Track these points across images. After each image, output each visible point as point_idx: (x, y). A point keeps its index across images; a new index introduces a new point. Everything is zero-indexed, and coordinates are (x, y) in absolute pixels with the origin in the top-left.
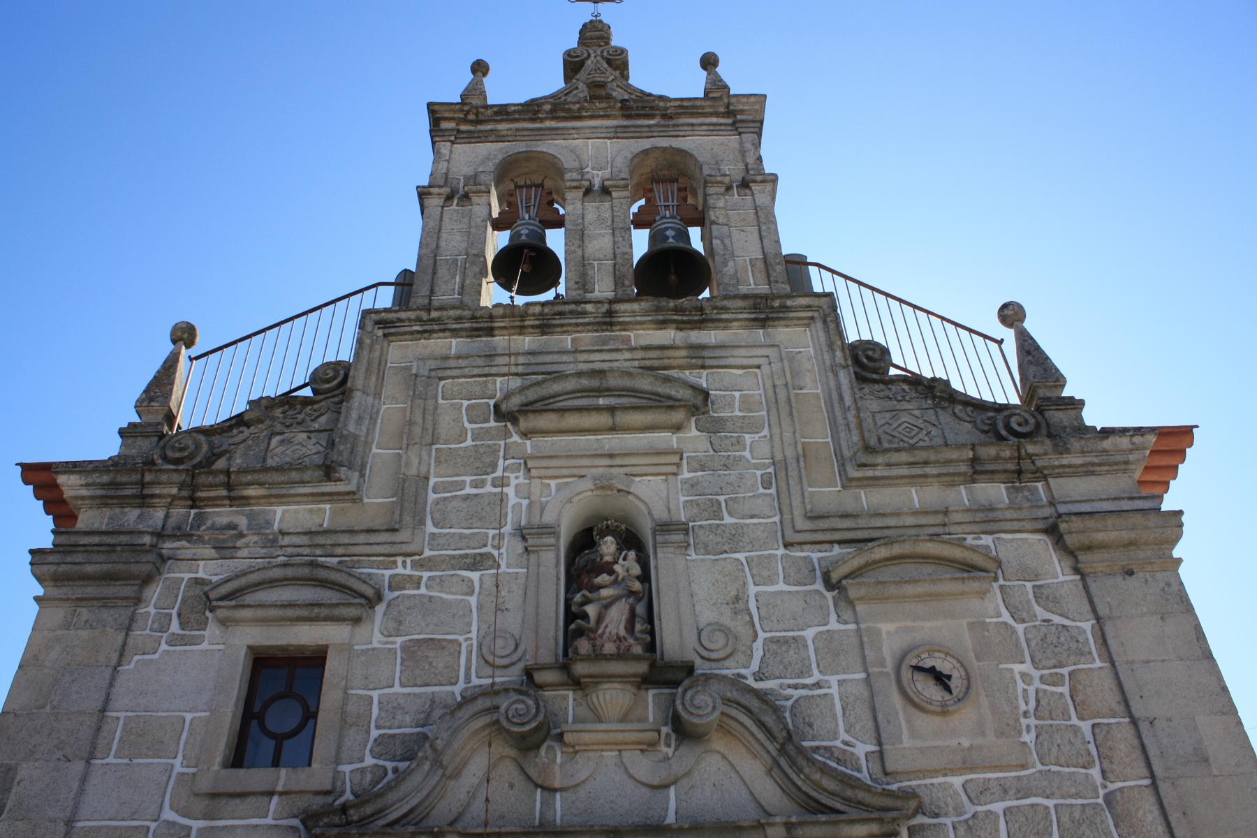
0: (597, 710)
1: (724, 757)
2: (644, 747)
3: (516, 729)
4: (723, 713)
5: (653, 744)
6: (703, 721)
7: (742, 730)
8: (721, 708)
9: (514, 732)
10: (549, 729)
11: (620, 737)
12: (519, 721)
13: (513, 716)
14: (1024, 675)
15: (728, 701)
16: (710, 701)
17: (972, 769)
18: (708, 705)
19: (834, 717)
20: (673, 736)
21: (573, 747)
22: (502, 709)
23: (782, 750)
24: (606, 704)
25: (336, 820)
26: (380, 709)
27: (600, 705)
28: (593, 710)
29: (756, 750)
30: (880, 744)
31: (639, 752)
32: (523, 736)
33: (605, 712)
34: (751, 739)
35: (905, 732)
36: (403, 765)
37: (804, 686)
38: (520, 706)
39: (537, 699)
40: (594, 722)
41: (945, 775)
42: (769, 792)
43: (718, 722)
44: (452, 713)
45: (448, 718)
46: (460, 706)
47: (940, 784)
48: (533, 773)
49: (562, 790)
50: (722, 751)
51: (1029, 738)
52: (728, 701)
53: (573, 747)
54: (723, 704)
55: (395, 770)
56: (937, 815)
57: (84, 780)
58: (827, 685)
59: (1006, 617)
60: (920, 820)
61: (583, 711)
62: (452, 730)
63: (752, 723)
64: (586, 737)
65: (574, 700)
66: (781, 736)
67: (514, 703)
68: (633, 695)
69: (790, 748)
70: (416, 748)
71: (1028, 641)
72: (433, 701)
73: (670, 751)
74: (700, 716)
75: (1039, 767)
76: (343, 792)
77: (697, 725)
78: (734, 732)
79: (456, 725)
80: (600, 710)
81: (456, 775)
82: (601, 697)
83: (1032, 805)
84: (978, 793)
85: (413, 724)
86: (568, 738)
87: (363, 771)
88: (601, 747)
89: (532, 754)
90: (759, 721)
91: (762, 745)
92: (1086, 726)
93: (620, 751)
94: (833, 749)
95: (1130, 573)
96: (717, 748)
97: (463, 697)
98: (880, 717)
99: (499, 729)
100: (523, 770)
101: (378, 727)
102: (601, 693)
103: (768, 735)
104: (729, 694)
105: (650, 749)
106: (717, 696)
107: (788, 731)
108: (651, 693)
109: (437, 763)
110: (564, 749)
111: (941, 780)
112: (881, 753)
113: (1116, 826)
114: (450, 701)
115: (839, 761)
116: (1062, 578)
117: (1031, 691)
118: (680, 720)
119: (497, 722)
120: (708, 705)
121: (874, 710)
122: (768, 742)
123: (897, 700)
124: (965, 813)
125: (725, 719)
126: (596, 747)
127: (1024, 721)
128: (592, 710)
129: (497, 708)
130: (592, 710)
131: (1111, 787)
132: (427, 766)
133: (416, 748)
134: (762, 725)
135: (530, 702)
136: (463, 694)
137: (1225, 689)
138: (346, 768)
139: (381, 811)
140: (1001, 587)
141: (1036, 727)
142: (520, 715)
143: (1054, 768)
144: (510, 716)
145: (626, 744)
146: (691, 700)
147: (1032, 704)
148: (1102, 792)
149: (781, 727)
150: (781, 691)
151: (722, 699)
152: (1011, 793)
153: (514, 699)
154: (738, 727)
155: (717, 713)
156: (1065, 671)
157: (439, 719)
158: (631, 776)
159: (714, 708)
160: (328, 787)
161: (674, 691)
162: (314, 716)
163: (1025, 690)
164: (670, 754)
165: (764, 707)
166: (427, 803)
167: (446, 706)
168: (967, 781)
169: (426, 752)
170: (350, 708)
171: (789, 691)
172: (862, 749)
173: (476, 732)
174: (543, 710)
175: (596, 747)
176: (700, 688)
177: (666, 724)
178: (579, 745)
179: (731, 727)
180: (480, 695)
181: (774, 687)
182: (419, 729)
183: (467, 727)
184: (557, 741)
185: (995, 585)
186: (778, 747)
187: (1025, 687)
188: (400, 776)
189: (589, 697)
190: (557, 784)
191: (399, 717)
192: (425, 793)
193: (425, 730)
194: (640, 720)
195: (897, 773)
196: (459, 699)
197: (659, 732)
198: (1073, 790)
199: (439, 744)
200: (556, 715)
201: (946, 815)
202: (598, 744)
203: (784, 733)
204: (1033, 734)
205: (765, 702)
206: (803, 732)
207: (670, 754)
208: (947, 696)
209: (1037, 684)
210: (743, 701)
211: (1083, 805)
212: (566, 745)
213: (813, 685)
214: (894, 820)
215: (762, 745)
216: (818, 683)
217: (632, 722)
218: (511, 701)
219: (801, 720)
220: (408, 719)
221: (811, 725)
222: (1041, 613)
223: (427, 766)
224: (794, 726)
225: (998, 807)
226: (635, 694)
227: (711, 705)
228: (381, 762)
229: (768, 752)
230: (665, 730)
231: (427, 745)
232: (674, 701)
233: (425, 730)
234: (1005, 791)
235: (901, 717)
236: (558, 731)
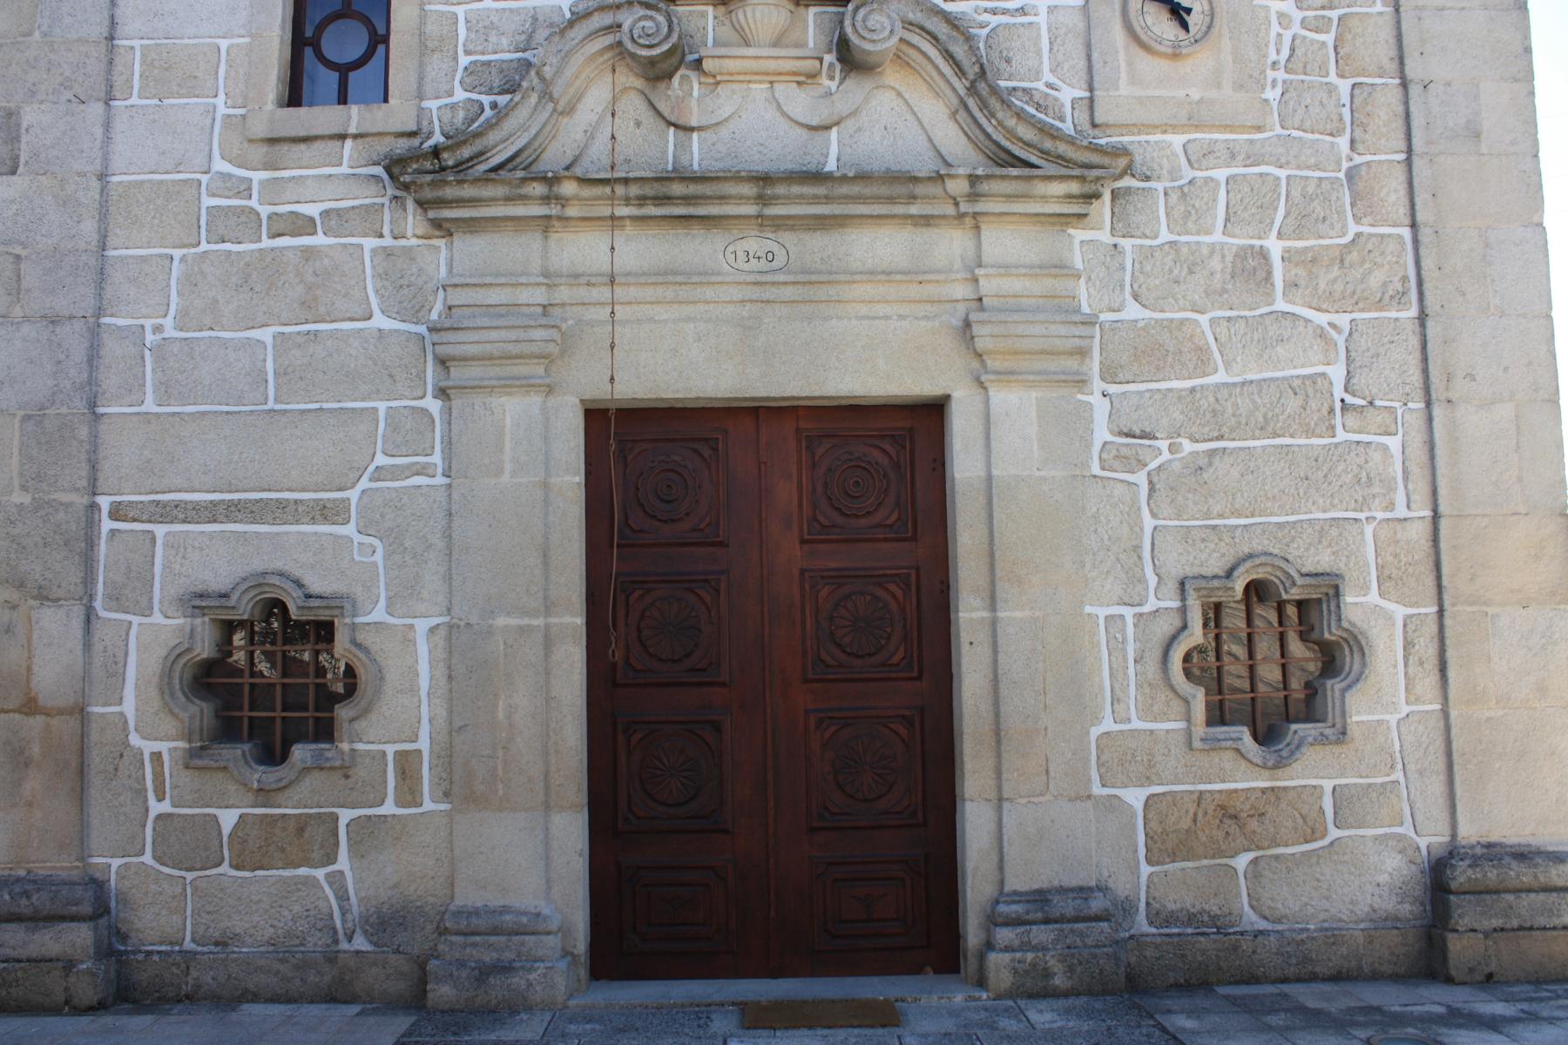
0: (743, 30)
1: (899, 94)
2: (802, 79)
3: (644, 52)
4: (901, 40)
5: (813, 76)
6: (878, 47)
7: (924, 62)
8: (900, 33)
9: (641, 56)
10: (683, 55)
11: (772, 65)
12: (647, 43)
13: (640, 37)
14: (1281, 16)
15: (909, 25)
16: (887, 23)
17: (1198, 127)
18: (885, 28)
19: (1039, 52)
20: (838, 67)
21: (714, 76)
22: (626, 27)
23: (972, 89)
24: (755, 21)
25: (428, 165)
26: (468, 29)
27: (748, 24)
28: (739, 30)
29: (940, 88)
30: (1091, 89)
31: (795, 85)
32: (652, 62)
33: (755, 34)
34: (934, 74)
35: (1124, 76)
36: (503, 100)
37: (1005, 12)
38: (648, 24)
39: (669, 15)
40: (740, 46)
41: (1165, 132)
42: (953, 140)
43: (894, 50)
44: (562, 32)
45: (557, 38)
46: (571, 24)
48: (663, 107)
49: (699, 129)
50: (897, 87)
51: (1272, 95)
52: (909, 25)
53: (714, 76)
54: (903, 28)
55: (494, 106)
56: (1147, 179)
57: (107, 126)
58: (1033, 12)
60: (1127, 182)
61: (726, 32)
62: (563, 53)
63: (937, 53)
64: (731, 65)
65: (715, 18)
66: (972, 71)
67: (640, 19)
68: (789, 14)
69: (982, 86)
70: (517, 77)
72: (535, 19)
73: (833, 85)
74: (874, 41)
75: (1279, 130)
76: (430, 134)
77: (869, 53)
78: (913, 64)
79: (567, 47)
80: (747, 31)
81: (570, 110)
82: (749, 15)
83: (1261, 175)
85: (512, 48)
86: (708, 65)
87: (453, 107)
88: (748, 78)
89: (662, 86)
90: (947, 51)
91: (948, 81)
92: (1344, 86)
93: (771, 83)
94: (1034, 92)
96: (892, 84)
97: (572, 13)
98: (1095, 55)
99: (621, 53)
100: (651, 104)
101: (467, 53)
102: (749, 9)
103: (956, 69)
104: (911, 16)
105: (809, 81)
106: (896, 16)
107: (982, 66)
108: (813, 10)
109: (546, 95)
110: (703, 80)
111: (1159, 137)
112: (1091, 100)
114: (557, 19)
115: (1038, 107)
117: (1287, 37)
118: (848, 46)
119: (620, 43)
120: (885, 28)
121: (1088, 46)
122: (956, 79)
123: (1118, 35)
124: (1182, 178)
125: (904, 47)
126: (741, 78)
127: (1270, 74)
128: (736, 30)
129: (619, 26)
130: (736, 30)
131: (1358, 160)
132: (534, 98)
133: (517, 77)
134: (949, 56)
135: (661, 18)
136: (573, 9)
138: (432, 104)
139: (482, 153)
141: (1284, 82)
142: (649, 35)
143: (1295, 133)
144: (635, 36)
145: (780, 74)
146: (864, 21)
147: (1285, 53)
148: (1345, 165)
149: (974, 60)
150: (976, 16)
151: (903, 22)
152: (1240, 158)
153: (640, 14)
154: (919, 58)
155: (895, 40)
156: (1334, 14)
157: (546, 40)
158: (784, 114)
159: (892, 31)
160: (414, 128)
161: (841, 9)
162: (385, 40)
163: (1279, 35)
164: (834, 89)
165: (955, 33)
166: (536, 144)
167: (551, 25)
168: (1189, 141)
169: (531, 81)
170: (429, 28)
171: (986, 17)
172: (1068, 94)
173: (592, 58)
174: (676, 28)
175: (741, 78)
176: (875, 6)
177: (830, 51)
178: (721, 74)
179: (911, 58)
180: (596, 10)
181: (968, 11)
182: (520, 55)
183: (582, 51)
184: (694, 70)
186: (968, 85)
187: (1281, 31)
188: (501, 114)
189: (733, 14)
190: (694, 123)
191: (493, 39)
192: (533, 132)
193: (527, 55)
194: (797, 45)
195: (1107, 126)
196: (568, 15)
197: (821, 60)
198: (1313, 161)
199: (548, 71)
200: (691, 37)
201: (1159, 178)
202: (745, 74)
203: (977, 68)
204: (1279, 90)
205: (955, 27)
206: (998, 70)
207: (834, 89)
208: (1182, 34)
209: (1296, 28)
210: (928, 25)
211: (1320, 179)
212: (704, 73)
213: (1017, 10)
214: (1098, 179)
215: (948, 81)
216: (1022, 8)
217: (787, 47)
218: (636, 16)
219: (997, 54)
220: (505, 41)
221: (1008, 61)
223: (534, 98)
224: (988, 61)
225: (1221, 174)
226: (792, 12)
227: (889, 28)
228: (475, 96)
229: (954, 90)
230: (829, 58)
231: (533, 73)
232: (841, 22)
233: (527, 55)
234: (1233, 156)
235: (1122, 55)
236: (696, 56)
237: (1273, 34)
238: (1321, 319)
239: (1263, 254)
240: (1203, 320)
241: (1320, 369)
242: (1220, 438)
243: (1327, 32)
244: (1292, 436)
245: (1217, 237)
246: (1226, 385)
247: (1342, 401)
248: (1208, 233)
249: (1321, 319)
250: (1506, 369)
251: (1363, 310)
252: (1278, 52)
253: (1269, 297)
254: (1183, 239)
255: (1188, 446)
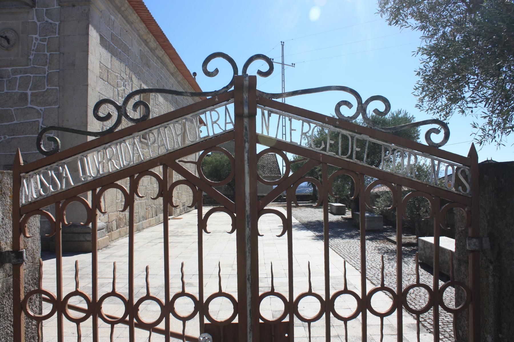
17: (13, 66)
41: (6, 67)
47: (5, 70)
56: (2, 78)
59: (35, 20)
71: (40, 27)
84: (15, 72)
92: (48, 54)
95: (74, 6)
111: (5, 68)
113: (47, 82)
116: (55, 7)
117: (37, 43)
124: (10, 77)
127: (32, 52)
131: (50, 71)
137: (88, 45)
140: (36, 10)
141: (35, 54)
147: (36, 47)
148: (47, 73)
156: (47, 37)
163: (35, 43)
168: (12, 69)
185: (34, 9)
187: (35, 42)
198: (39, 72)
201: (5, 78)
204: (33, 56)
211: (40, 76)
222: (46, 18)
234: (21, 72)
237: (33, 43)
238: (38, 108)
239: (26, 94)
240: (12, 109)
241: (37, 119)
242: (14, 135)
243: (46, 42)
244: (29, 134)
245: (16, 91)
246: (16, 124)
247: (41, 126)
248: (14, 90)
249: (38, 108)
250: (76, 119)
251: (46, 106)
252: (34, 47)
253: (27, 104)
254: (9, 91)
255: (7, 137)
